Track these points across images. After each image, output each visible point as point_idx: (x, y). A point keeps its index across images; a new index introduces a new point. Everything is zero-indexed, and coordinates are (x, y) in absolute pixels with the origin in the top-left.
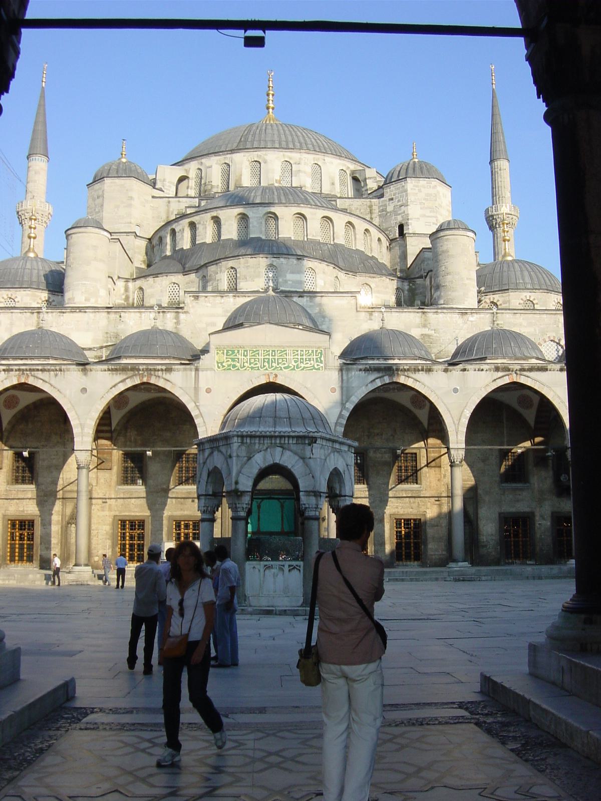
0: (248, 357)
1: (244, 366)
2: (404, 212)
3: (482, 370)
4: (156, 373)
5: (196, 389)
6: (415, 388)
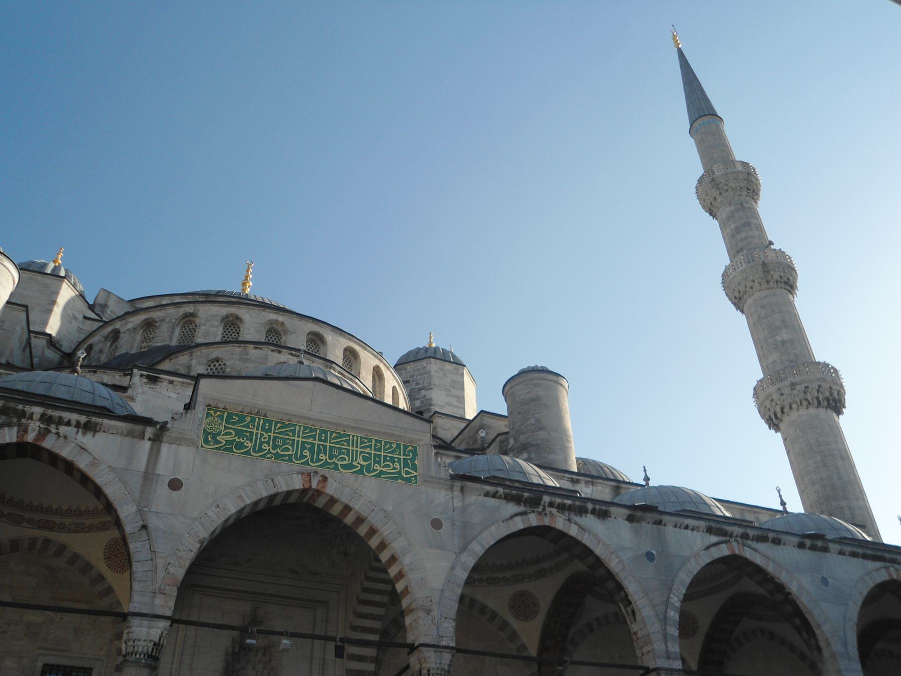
0: (272, 434)
1: (262, 450)
2: (425, 396)
3: (687, 527)
4: (63, 429)
5: (149, 476)
6: (584, 541)
